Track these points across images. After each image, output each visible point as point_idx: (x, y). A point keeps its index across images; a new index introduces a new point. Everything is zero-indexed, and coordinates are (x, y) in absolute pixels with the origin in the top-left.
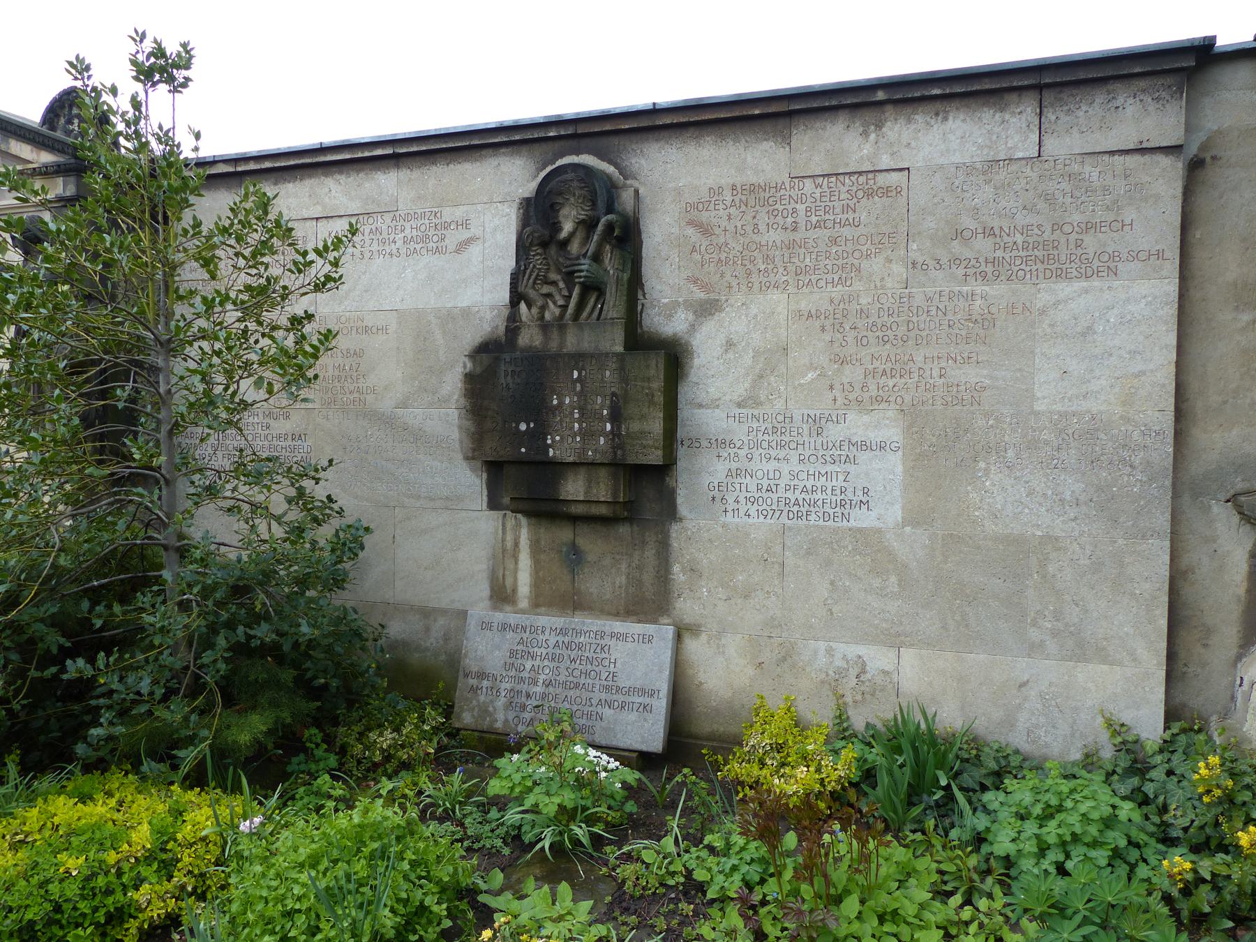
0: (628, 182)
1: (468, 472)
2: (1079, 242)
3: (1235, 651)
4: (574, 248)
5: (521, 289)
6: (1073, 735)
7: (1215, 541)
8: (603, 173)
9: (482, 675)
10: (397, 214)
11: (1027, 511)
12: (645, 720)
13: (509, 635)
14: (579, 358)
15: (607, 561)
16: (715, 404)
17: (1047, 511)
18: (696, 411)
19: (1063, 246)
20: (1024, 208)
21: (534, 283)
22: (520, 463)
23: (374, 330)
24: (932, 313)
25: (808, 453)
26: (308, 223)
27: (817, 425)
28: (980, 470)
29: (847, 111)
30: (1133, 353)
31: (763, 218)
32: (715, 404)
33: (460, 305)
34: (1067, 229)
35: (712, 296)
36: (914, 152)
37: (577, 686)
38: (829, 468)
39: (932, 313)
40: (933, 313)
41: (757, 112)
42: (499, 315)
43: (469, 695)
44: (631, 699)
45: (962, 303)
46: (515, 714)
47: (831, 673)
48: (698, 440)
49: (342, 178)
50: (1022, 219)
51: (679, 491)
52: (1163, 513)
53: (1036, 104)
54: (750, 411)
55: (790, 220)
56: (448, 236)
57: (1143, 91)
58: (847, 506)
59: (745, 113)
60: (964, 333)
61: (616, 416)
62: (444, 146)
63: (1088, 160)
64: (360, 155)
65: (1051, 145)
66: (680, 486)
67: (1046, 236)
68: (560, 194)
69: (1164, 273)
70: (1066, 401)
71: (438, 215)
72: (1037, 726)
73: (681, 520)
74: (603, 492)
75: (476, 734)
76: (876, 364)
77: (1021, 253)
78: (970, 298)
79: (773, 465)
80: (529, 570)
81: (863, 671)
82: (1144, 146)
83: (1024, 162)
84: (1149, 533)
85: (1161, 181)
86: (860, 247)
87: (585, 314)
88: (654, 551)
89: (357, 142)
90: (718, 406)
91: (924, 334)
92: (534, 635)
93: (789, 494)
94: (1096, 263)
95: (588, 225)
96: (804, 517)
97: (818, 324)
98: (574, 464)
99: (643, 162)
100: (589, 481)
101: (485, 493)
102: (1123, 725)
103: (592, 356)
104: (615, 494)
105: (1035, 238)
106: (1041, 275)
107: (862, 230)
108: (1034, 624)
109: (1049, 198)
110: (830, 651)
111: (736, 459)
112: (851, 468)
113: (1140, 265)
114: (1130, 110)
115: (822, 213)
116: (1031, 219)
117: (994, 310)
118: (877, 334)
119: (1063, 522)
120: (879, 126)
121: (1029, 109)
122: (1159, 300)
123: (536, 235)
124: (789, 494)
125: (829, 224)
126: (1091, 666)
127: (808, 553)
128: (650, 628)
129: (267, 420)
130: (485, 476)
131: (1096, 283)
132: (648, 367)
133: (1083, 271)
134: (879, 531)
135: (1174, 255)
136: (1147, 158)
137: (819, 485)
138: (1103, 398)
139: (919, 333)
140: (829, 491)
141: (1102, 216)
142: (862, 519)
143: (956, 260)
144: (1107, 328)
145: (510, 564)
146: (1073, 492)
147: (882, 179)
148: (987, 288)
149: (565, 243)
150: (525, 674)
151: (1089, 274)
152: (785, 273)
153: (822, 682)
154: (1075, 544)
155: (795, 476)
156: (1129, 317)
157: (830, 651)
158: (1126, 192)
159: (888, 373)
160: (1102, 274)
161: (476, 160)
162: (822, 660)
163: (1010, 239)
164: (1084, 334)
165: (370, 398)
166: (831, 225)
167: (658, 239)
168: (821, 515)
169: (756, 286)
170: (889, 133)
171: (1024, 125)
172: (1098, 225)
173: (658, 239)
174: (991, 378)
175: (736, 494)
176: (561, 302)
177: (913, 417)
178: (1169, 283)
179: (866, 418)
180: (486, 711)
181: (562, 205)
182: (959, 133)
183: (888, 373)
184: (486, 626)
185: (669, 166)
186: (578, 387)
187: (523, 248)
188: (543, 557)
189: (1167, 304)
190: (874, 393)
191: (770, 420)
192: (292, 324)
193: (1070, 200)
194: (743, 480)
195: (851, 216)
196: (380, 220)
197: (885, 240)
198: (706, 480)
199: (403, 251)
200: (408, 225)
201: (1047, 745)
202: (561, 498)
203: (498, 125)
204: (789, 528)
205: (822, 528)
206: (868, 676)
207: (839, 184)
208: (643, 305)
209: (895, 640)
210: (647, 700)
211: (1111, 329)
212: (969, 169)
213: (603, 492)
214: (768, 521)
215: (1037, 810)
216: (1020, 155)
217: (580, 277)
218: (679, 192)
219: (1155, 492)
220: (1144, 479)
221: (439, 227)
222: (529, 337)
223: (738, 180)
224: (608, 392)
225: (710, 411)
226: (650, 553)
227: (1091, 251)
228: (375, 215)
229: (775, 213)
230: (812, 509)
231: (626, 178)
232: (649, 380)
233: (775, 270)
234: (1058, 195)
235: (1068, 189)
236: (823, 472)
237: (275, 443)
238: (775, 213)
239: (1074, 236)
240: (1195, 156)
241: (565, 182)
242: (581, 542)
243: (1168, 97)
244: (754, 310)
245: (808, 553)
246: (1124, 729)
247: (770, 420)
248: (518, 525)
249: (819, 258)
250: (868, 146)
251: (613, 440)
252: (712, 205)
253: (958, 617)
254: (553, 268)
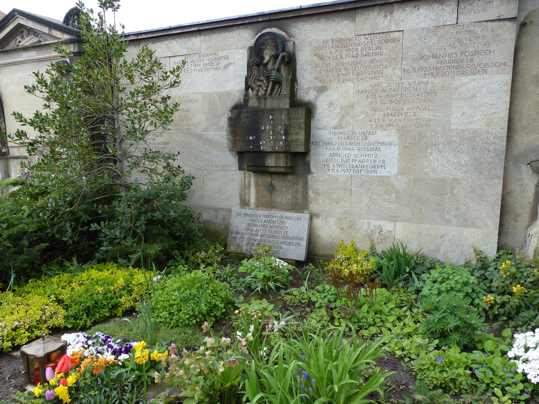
0: (291, 39)
1: (231, 156)
3: (527, 223)
4: (270, 66)
5: (249, 83)
6: (461, 255)
7: (522, 180)
8: (281, 35)
9: (237, 233)
10: (201, 54)
11: (446, 169)
12: (298, 249)
13: (247, 218)
14: (272, 111)
15: (284, 190)
16: (325, 128)
18: (318, 131)
19: (465, 61)
20: (450, 46)
21: (254, 81)
22: (250, 152)
23: (193, 101)
24: (411, 90)
25: (361, 147)
26: (167, 59)
27: (365, 136)
28: (428, 153)
29: (378, 7)
30: (492, 105)
31: (344, 52)
32: (325, 128)
33: (226, 90)
34: (467, 54)
35: (324, 85)
36: (405, 23)
37: (273, 236)
38: (370, 152)
39: (411, 90)
40: (411, 90)
41: (342, 8)
42: (241, 94)
43: (233, 240)
44: (293, 241)
45: (423, 86)
46: (250, 247)
47: (369, 231)
48: (318, 142)
49: (179, 40)
50: (449, 50)
51: (311, 162)
52: (500, 170)
54: (339, 131)
55: (355, 53)
56: (221, 63)
58: (376, 167)
59: (337, 9)
60: (423, 98)
61: (286, 133)
62: (218, 26)
63: (477, 24)
64: (185, 31)
65: (462, 18)
66: (312, 160)
67: (458, 57)
68: (264, 45)
69: (506, 71)
71: (217, 54)
72: (447, 252)
73: (312, 173)
74: (282, 163)
75: (236, 254)
76: (389, 111)
77: (448, 65)
78: (426, 84)
79: (348, 152)
80: (254, 193)
81: (381, 231)
82: (501, 18)
83: (450, 26)
84: (495, 177)
85: (507, 33)
86: (382, 64)
87: (274, 93)
88: (302, 186)
89: (184, 25)
90: (326, 129)
91: (408, 98)
92: (257, 218)
93: (354, 163)
94: (478, 68)
95: (275, 57)
96: (359, 172)
97: (366, 95)
98: (271, 152)
99: (297, 30)
100: (277, 159)
101: (237, 164)
102: (481, 251)
103: (277, 110)
104: (286, 163)
105: (454, 58)
107: (384, 56)
108: (448, 213)
109: (459, 41)
110: (369, 223)
111: (333, 149)
112: (377, 152)
113: (496, 68)
115: (368, 50)
116: (453, 50)
117: (436, 88)
118: (389, 99)
119: (460, 173)
120: (391, 13)
121: (453, 4)
122: (503, 83)
123: (255, 61)
124: (354, 163)
125: (371, 54)
126: (469, 229)
127: (361, 186)
128: (300, 215)
129: (154, 137)
130: (237, 157)
131: (478, 76)
132: (298, 114)
133: (473, 71)
134: (388, 177)
136: (502, 23)
137: (365, 159)
138: (479, 123)
139: (405, 98)
140: (369, 162)
142: (382, 172)
143: (421, 68)
145: (247, 191)
146: (465, 161)
147: (392, 35)
148: (433, 79)
149: (266, 65)
150: (253, 232)
151: (475, 72)
152: (353, 75)
153: (366, 235)
155: (356, 156)
157: (369, 223)
159: (393, 114)
160: (481, 73)
161: (231, 31)
162: (366, 227)
163: (443, 59)
164: (472, 98)
165: (193, 128)
166: (371, 55)
167: (303, 62)
168: (366, 171)
169: (342, 80)
170: (396, 16)
171: (451, 11)
173: (303, 62)
174: (433, 116)
175: (333, 163)
176: (265, 88)
177: (403, 132)
179: (384, 133)
180: (239, 246)
181: (265, 49)
182: (424, 15)
183: (393, 114)
184: (239, 214)
185: (307, 32)
186: (272, 122)
187: (249, 67)
188: (260, 188)
189: (507, 84)
190: (387, 123)
191: (346, 134)
192: (163, 100)
193: (469, 42)
194: (336, 158)
195: (379, 51)
196: (194, 57)
197: (393, 61)
198: (322, 158)
199: (203, 69)
200: (205, 59)
201: (451, 259)
202: (266, 165)
203: (239, 17)
204: (354, 176)
205: (366, 176)
206: (383, 233)
207: (375, 37)
208: (297, 89)
209: (394, 219)
210: (299, 242)
211: (483, 95)
212: (428, 30)
213: (282, 163)
214: (346, 173)
215: (440, 280)
216: (449, 23)
217: (272, 78)
218: (311, 42)
219: (498, 161)
220: (494, 156)
221: (217, 59)
222: (253, 103)
223: (334, 37)
224: (283, 124)
225: (323, 131)
226: (300, 186)
227: (476, 63)
228: (192, 55)
229: (349, 50)
230: (363, 169)
231: (290, 37)
232: (299, 119)
233: (349, 74)
234: (464, 40)
235: (468, 37)
236: (367, 154)
237: (157, 146)
238: (349, 50)
239: (470, 57)
240: (523, 21)
241: (266, 40)
242: (274, 182)
244: (341, 90)
245: (361, 186)
246: (481, 253)
247: (346, 134)
248: (250, 176)
249: (367, 68)
250: (386, 21)
251: (285, 142)
252: (324, 48)
253: (418, 210)
254: (261, 75)
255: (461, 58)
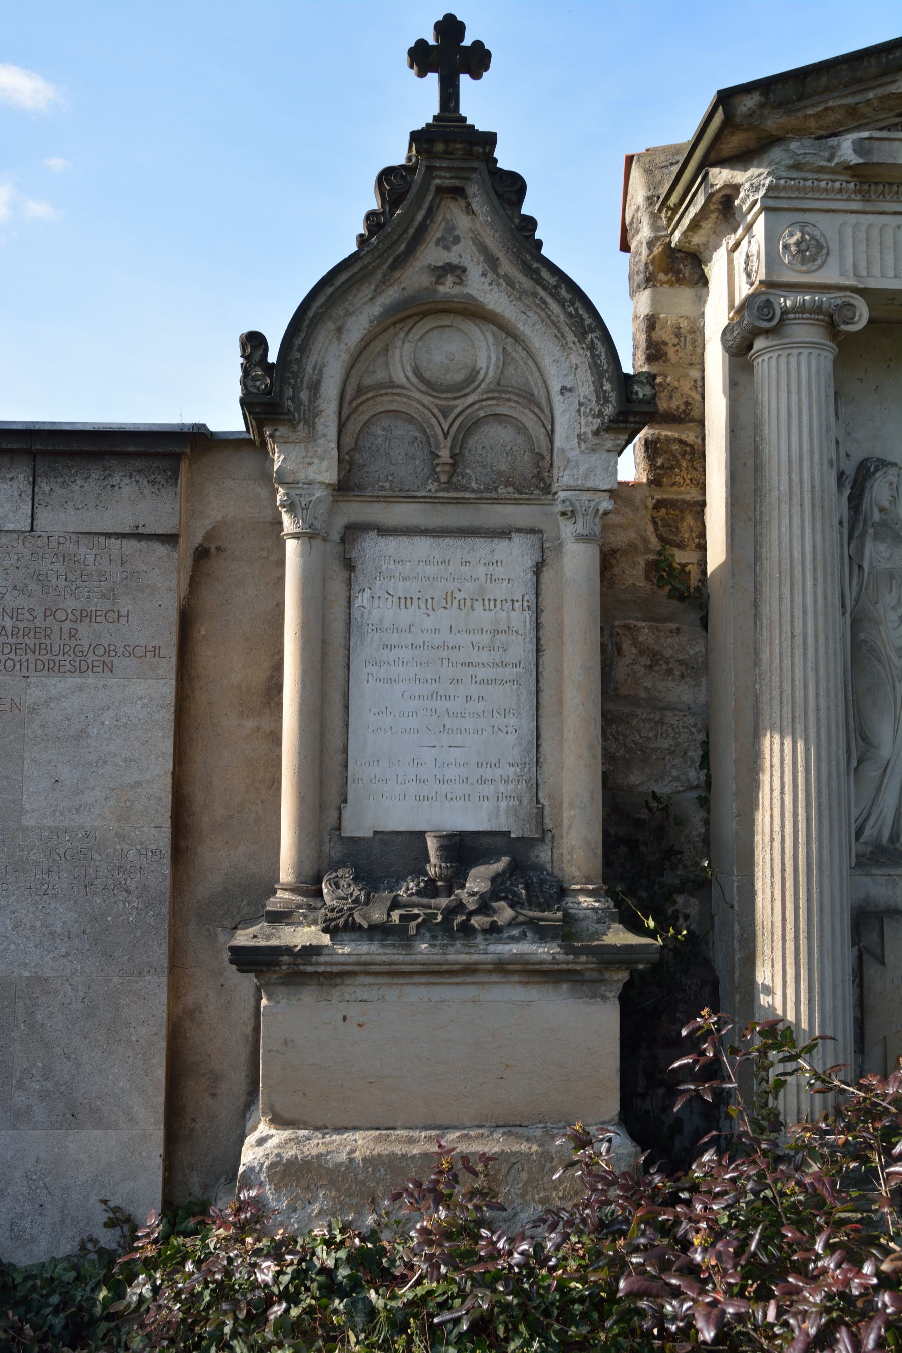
2: (73, 632)
6: (62, 1222)
11: (12, 947)
17: (36, 946)
19: (56, 635)
20: (14, 588)
34: (61, 615)
52: (160, 945)
53: (29, 471)
57: (139, 471)
63: (83, 540)
65: (44, 518)
67: (37, 622)
70: (58, 814)
77: (10, 640)
82: (141, 530)
83: (14, 535)
85: (157, 571)
94: (91, 657)
106: (32, 667)
108: (20, 1086)
109: (39, 578)
114: (126, 490)
116: (21, 602)
119: (54, 959)
121: (21, 476)
122: (155, 703)
131: (91, 679)
135: (171, 653)
138: (97, 812)
141: (97, 604)
144: (102, 731)
146: (64, 923)
151: (84, 668)
154: (66, 985)
156: (124, 720)
158: (122, 579)
160: (98, 670)
164: (77, 738)
171: (15, 494)
172: (93, 613)
178: (165, 684)
189: (163, 707)
193: (64, 583)
211: (106, 732)
216: (11, 527)
220: (141, 906)
227: (85, 643)
234: (52, 577)
239: (67, 625)
243: (163, 482)
255: (44, 625)
